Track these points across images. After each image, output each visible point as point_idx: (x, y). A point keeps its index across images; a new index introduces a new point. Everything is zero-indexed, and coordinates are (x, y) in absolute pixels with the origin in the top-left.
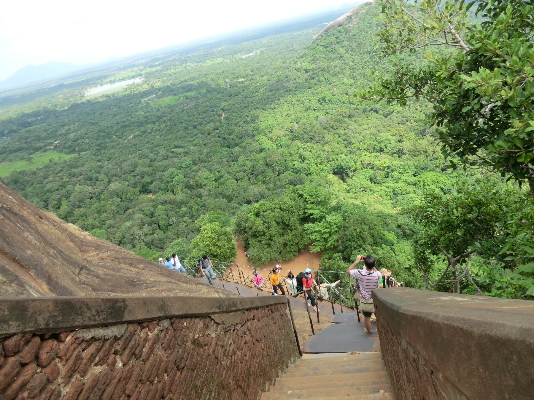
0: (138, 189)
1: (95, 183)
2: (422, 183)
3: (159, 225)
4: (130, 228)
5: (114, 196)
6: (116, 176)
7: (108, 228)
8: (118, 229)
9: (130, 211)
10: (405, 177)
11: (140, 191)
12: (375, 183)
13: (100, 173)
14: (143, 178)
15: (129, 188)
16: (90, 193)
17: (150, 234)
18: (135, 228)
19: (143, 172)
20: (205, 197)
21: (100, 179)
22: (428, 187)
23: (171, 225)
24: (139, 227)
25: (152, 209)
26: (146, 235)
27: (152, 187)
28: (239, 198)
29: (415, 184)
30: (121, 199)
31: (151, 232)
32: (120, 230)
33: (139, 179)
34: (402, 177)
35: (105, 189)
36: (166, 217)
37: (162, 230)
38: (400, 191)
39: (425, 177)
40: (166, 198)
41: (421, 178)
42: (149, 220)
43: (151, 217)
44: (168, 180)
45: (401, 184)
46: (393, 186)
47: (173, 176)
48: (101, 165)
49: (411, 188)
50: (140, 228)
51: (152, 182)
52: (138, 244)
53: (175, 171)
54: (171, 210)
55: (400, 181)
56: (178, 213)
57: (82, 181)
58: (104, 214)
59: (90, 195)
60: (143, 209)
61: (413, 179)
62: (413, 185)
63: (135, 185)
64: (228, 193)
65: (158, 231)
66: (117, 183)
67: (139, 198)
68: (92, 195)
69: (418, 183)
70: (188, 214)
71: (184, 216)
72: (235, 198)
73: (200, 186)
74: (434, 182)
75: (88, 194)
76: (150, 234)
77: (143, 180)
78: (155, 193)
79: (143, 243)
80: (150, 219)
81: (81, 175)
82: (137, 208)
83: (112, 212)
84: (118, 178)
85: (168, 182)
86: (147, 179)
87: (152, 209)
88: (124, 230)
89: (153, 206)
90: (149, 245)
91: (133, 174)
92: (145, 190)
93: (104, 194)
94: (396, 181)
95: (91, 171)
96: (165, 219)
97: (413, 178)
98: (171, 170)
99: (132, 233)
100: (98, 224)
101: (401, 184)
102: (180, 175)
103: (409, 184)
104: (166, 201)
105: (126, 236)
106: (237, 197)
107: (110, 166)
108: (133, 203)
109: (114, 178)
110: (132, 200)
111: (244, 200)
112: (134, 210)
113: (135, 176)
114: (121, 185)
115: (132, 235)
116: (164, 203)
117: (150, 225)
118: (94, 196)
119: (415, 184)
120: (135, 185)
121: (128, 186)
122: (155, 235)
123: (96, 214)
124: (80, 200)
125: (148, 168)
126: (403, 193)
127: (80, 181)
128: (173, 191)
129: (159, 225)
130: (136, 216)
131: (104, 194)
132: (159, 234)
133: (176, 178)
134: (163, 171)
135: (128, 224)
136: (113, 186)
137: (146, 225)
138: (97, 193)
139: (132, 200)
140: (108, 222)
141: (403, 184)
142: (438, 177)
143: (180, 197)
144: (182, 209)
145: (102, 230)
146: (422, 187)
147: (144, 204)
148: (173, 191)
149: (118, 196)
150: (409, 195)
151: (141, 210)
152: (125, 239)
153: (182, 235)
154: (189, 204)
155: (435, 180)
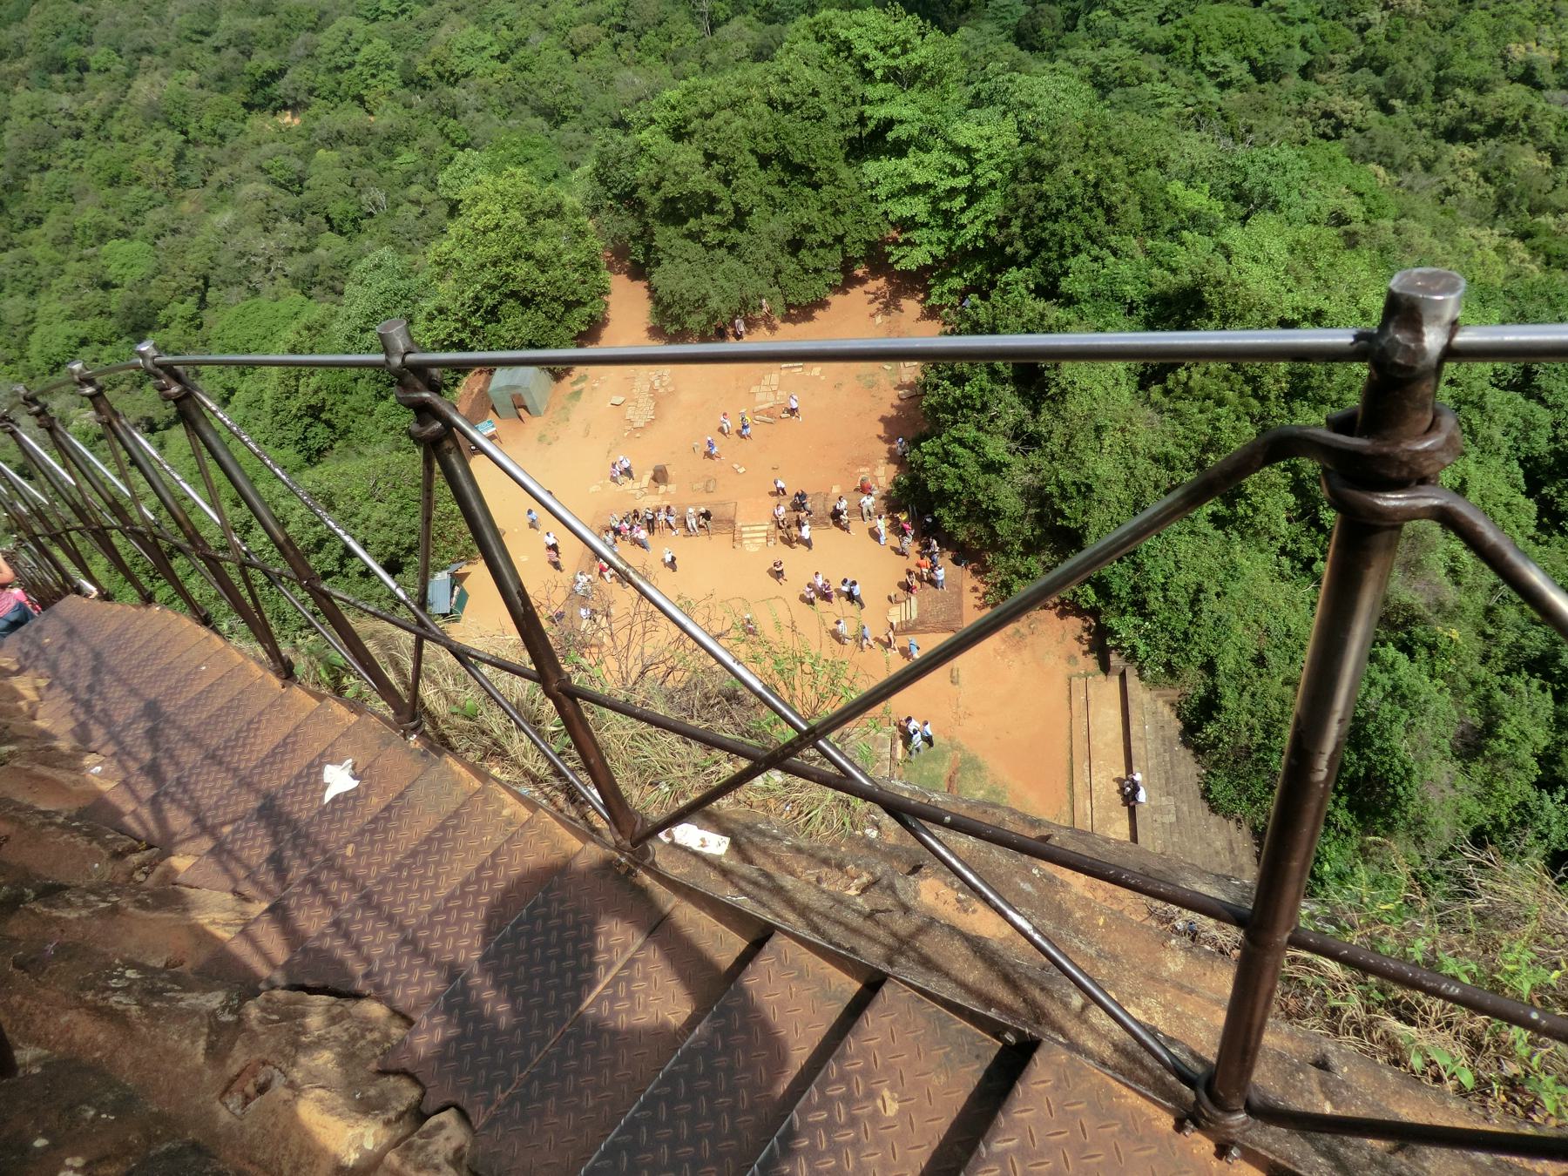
0: (239, 93)
1: (79, 80)
2: (1189, 45)
3: (328, 220)
4: (231, 230)
5: (157, 124)
6: (148, 50)
7: (157, 237)
8: (193, 236)
9: (222, 174)
10: (1132, 26)
11: (245, 105)
12: (1032, 49)
13: (90, 42)
14: (248, 55)
15: (204, 93)
16: (72, 117)
17: (302, 250)
18: (247, 232)
19: (243, 35)
20: (471, 113)
21: (94, 66)
22: (1210, 58)
23: (371, 215)
24: (260, 227)
25: (298, 165)
26: (290, 251)
27: (281, 88)
28: (587, 112)
29: (1166, 49)
30: (185, 133)
31: (303, 242)
32: (199, 239)
33: (235, 60)
34: (1122, 26)
35: (120, 102)
36: (349, 190)
37: (341, 233)
38: (1117, 74)
39: (1200, 22)
40: (339, 126)
41: (1187, 27)
42: (291, 201)
43: (299, 193)
44: (341, 62)
45: (1118, 50)
46: (1094, 57)
47: (353, 44)
48: (89, 15)
49: (1152, 64)
50: (266, 230)
51: (282, 72)
52: (268, 284)
53: (360, 27)
54: (360, 165)
55: (1118, 41)
56: (387, 175)
57: (34, 75)
58: (135, 190)
59: (73, 124)
60: (265, 165)
61: (1158, 34)
62: (1160, 52)
63: (222, 81)
64: (547, 97)
65: (330, 238)
66: (157, 76)
67: (247, 128)
68: (80, 123)
69: (1177, 44)
70: (421, 176)
71: (408, 183)
72: (571, 113)
73: (452, 78)
74: (1229, 41)
75: (66, 122)
76: (302, 250)
77: (248, 65)
78: (296, 107)
79: (283, 281)
80: (297, 200)
81: (21, 53)
82: (245, 164)
83: (162, 180)
84: (158, 60)
85: (339, 69)
86: (265, 61)
87: (298, 165)
88: (213, 237)
89: (298, 155)
90: (306, 284)
91: (208, 41)
92: (263, 95)
93: (121, 120)
94: (1099, 40)
95: (58, 35)
96: (345, 195)
97: (1156, 28)
98: (343, 22)
99: (240, 247)
100: (121, 225)
101: (1118, 50)
102: (376, 41)
103: (1146, 49)
104: (340, 135)
105: (223, 261)
106: (578, 110)
107: (121, 17)
108: (228, 146)
109: (146, 58)
110: (222, 137)
111: (606, 120)
112: (236, 169)
113: (217, 50)
114: (171, 84)
115: (242, 255)
116: (336, 139)
117: (297, 217)
118: (84, 126)
119: (1166, 49)
120: (222, 81)
121: (201, 86)
122: (320, 251)
123: (109, 191)
124: (41, 141)
125: (260, 20)
126: (1127, 80)
127: (24, 74)
128: (360, 100)
129: (328, 220)
130: (246, 190)
131: (121, 120)
132: (330, 246)
133: (366, 51)
134: (315, 29)
135: (225, 217)
136: (144, 89)
137: (285, 219)
138: (96, 115)
139: (222, 137)
140: (154, 217)
141: (1126, 51)
142: (1243, 22)
143: (385, 118)
144: (399, 160)
145: (137, 244)
146: (1188, 60)
147: (266, 149)
148: (360, 100)
149: (171, 125)
150: (1148, 86)
151: (260, 168)
152: (219, 271)
153: (408, 245)
154: (421, 142)
155: (1232, 31)
